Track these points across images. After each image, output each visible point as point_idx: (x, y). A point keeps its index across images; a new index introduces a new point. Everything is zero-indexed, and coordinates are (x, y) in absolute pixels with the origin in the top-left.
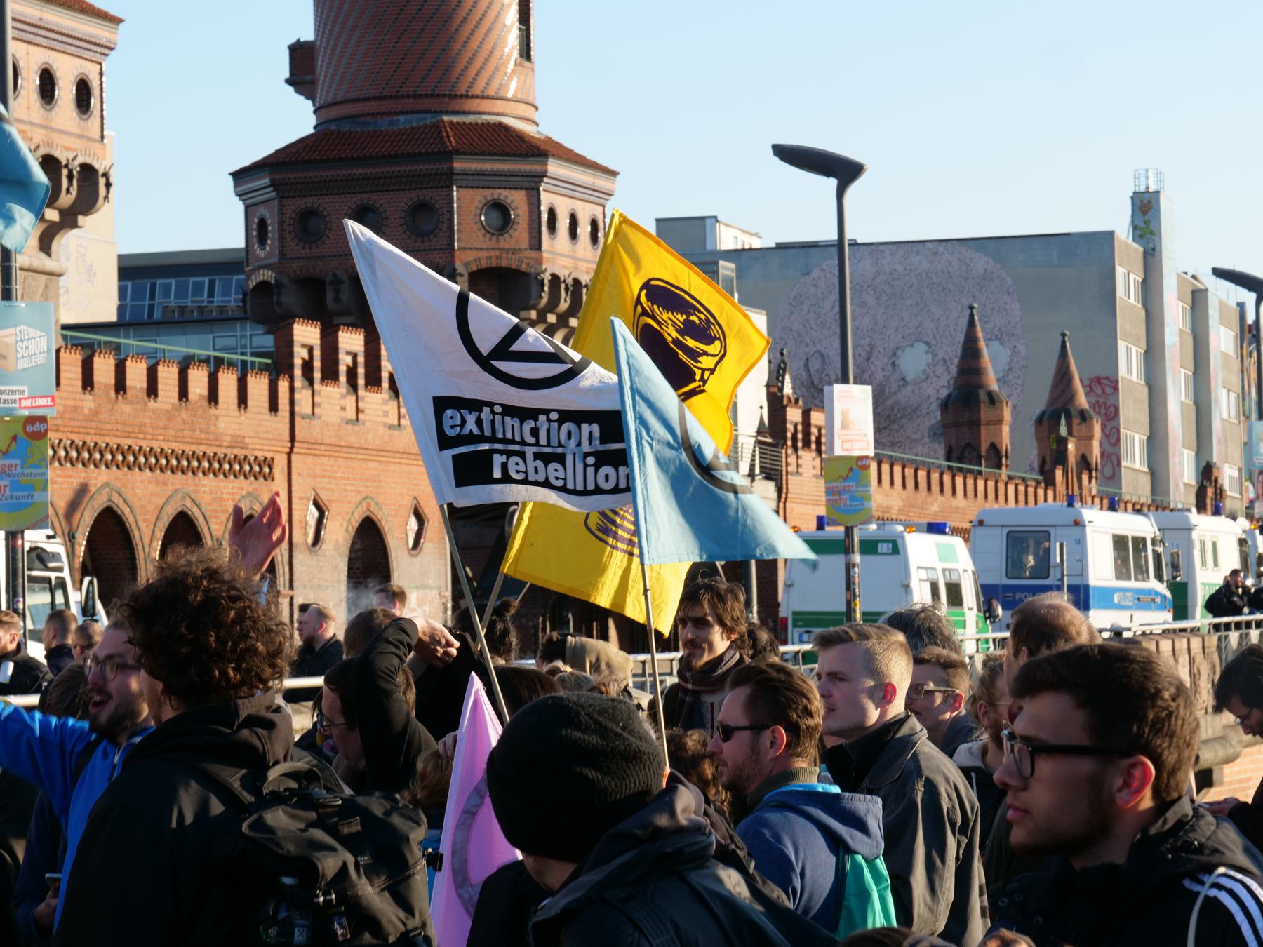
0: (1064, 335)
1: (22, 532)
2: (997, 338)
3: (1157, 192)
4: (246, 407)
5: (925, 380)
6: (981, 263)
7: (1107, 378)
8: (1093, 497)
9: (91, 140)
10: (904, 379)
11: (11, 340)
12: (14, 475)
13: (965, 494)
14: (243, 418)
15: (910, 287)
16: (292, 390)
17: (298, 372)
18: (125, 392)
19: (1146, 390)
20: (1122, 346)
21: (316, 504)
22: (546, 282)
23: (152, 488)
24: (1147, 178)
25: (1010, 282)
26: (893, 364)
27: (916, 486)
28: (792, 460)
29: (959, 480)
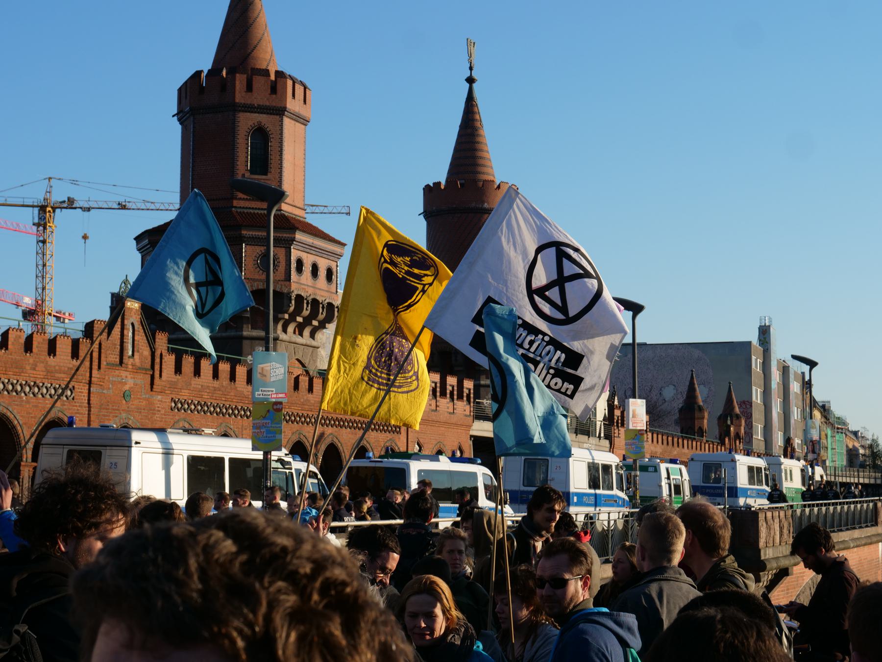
0: (730, 383)
1: (271, 452)
3: (769, 326)
5: (673, 401)
7: (748, 401)
8: (741, 450)
9: (332, 293)
11: (268, 368)
13: (688, 448)
19: (763, 407)
20: (754, 388)
21: (418, 444)
23: (350, 436)
24: (765, 320)
25: (708, 361)
27: (668, 443)
29: (685, 442)
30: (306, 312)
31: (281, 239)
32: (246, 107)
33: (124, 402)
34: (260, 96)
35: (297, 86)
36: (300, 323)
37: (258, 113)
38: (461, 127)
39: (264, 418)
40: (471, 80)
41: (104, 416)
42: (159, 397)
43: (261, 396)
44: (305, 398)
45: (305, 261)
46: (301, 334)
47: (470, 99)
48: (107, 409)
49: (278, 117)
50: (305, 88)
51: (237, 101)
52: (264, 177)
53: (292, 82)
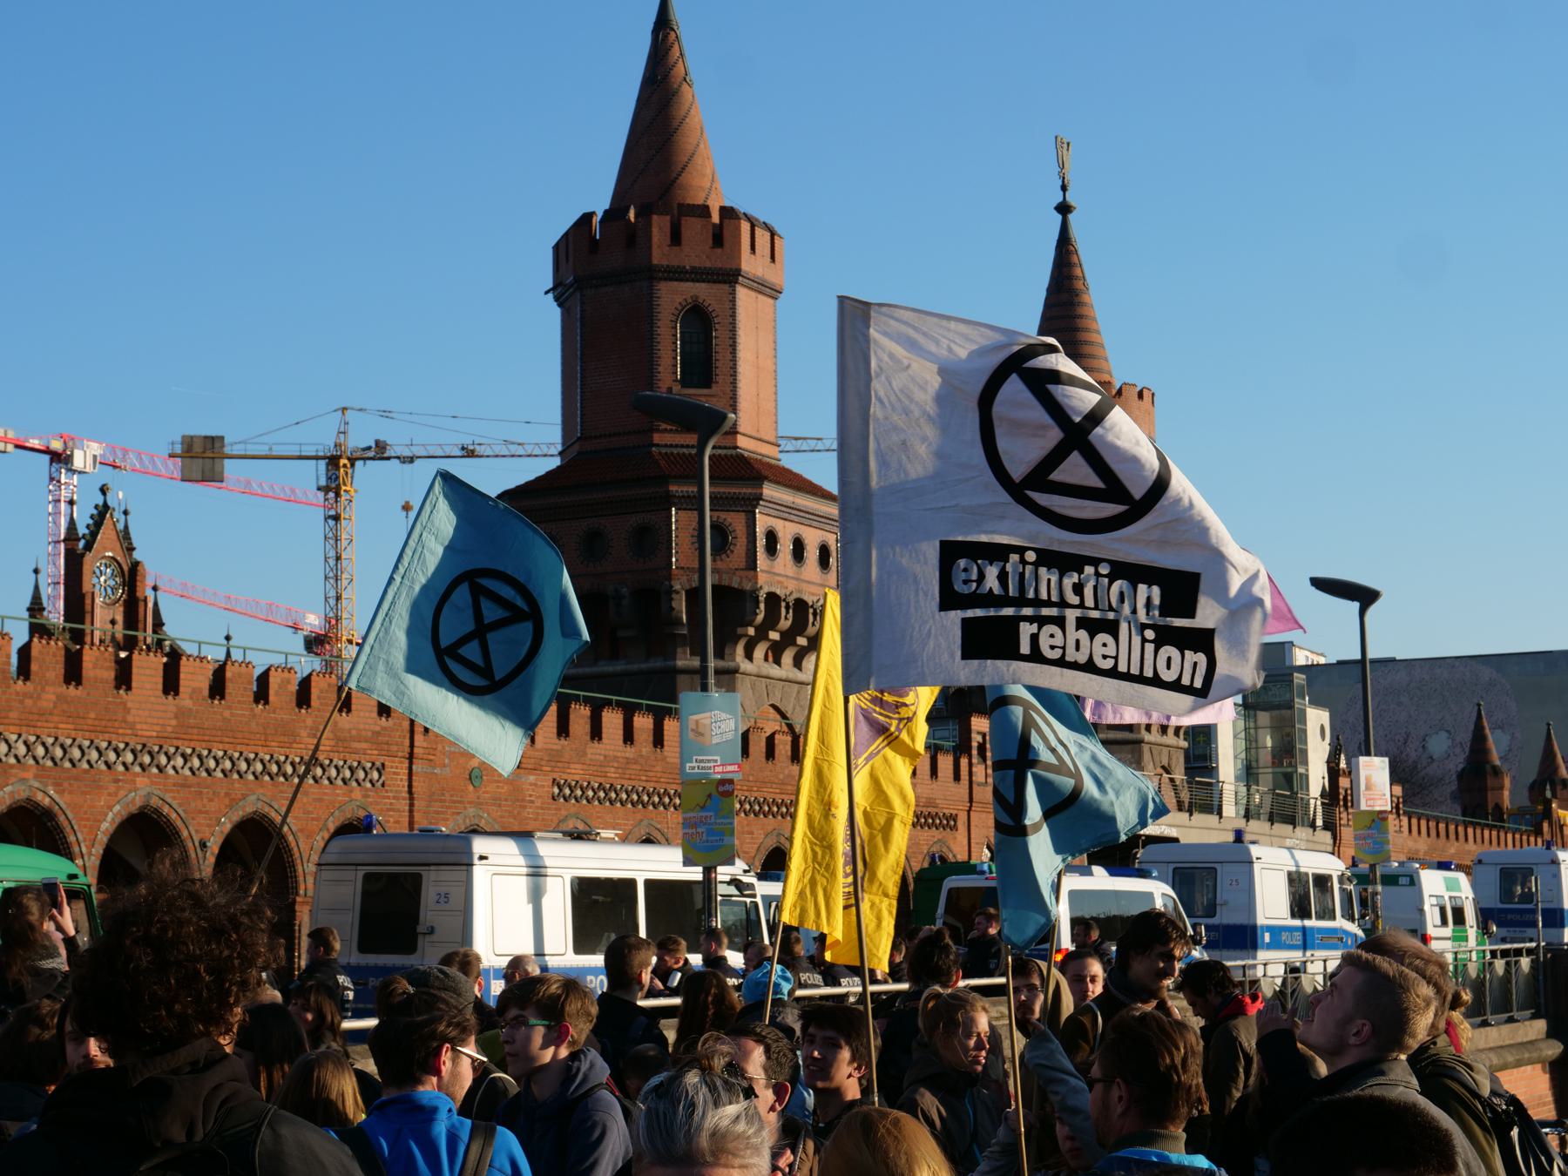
0: (1549, 725)
1: (715, 868)
2: (1500, 727)
4: (937, 777)
5: (1447, 758)
6: (1487, 673)
10: (1431, 757)
11: (707, 722)
12: (710, 824)
13: (1475, 841)
14: (935, 785)
15: (1435, 690)
16: (970, 765)
17: (975, 752)
18: (774, 758)
22: (762, 599)
26: (1423, 746)
27: (1438, 835)
28: (1344, 815)
29: (1470, 831)
30: (785, 624)
31: (738, 498)
32: (670, 272)
33: (471, 788)
34: (695, 252)
35: (759, 232)
36: (775, 643)
37: (693, 281)
38: (1049, 290)
39: (703, 808)
40: (1064, 209)
41: (437, 813)
42: (532, 778)
43: (696, 770)
44: (786, 772)
45: (780, 535)
46: (778, 662)
47: (1064, 242)
48: (441, 801)
49: (726, 287)
50: (773, 234)
51: (655, 262)
52: (705, 391)
53: (749, 225)
